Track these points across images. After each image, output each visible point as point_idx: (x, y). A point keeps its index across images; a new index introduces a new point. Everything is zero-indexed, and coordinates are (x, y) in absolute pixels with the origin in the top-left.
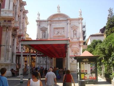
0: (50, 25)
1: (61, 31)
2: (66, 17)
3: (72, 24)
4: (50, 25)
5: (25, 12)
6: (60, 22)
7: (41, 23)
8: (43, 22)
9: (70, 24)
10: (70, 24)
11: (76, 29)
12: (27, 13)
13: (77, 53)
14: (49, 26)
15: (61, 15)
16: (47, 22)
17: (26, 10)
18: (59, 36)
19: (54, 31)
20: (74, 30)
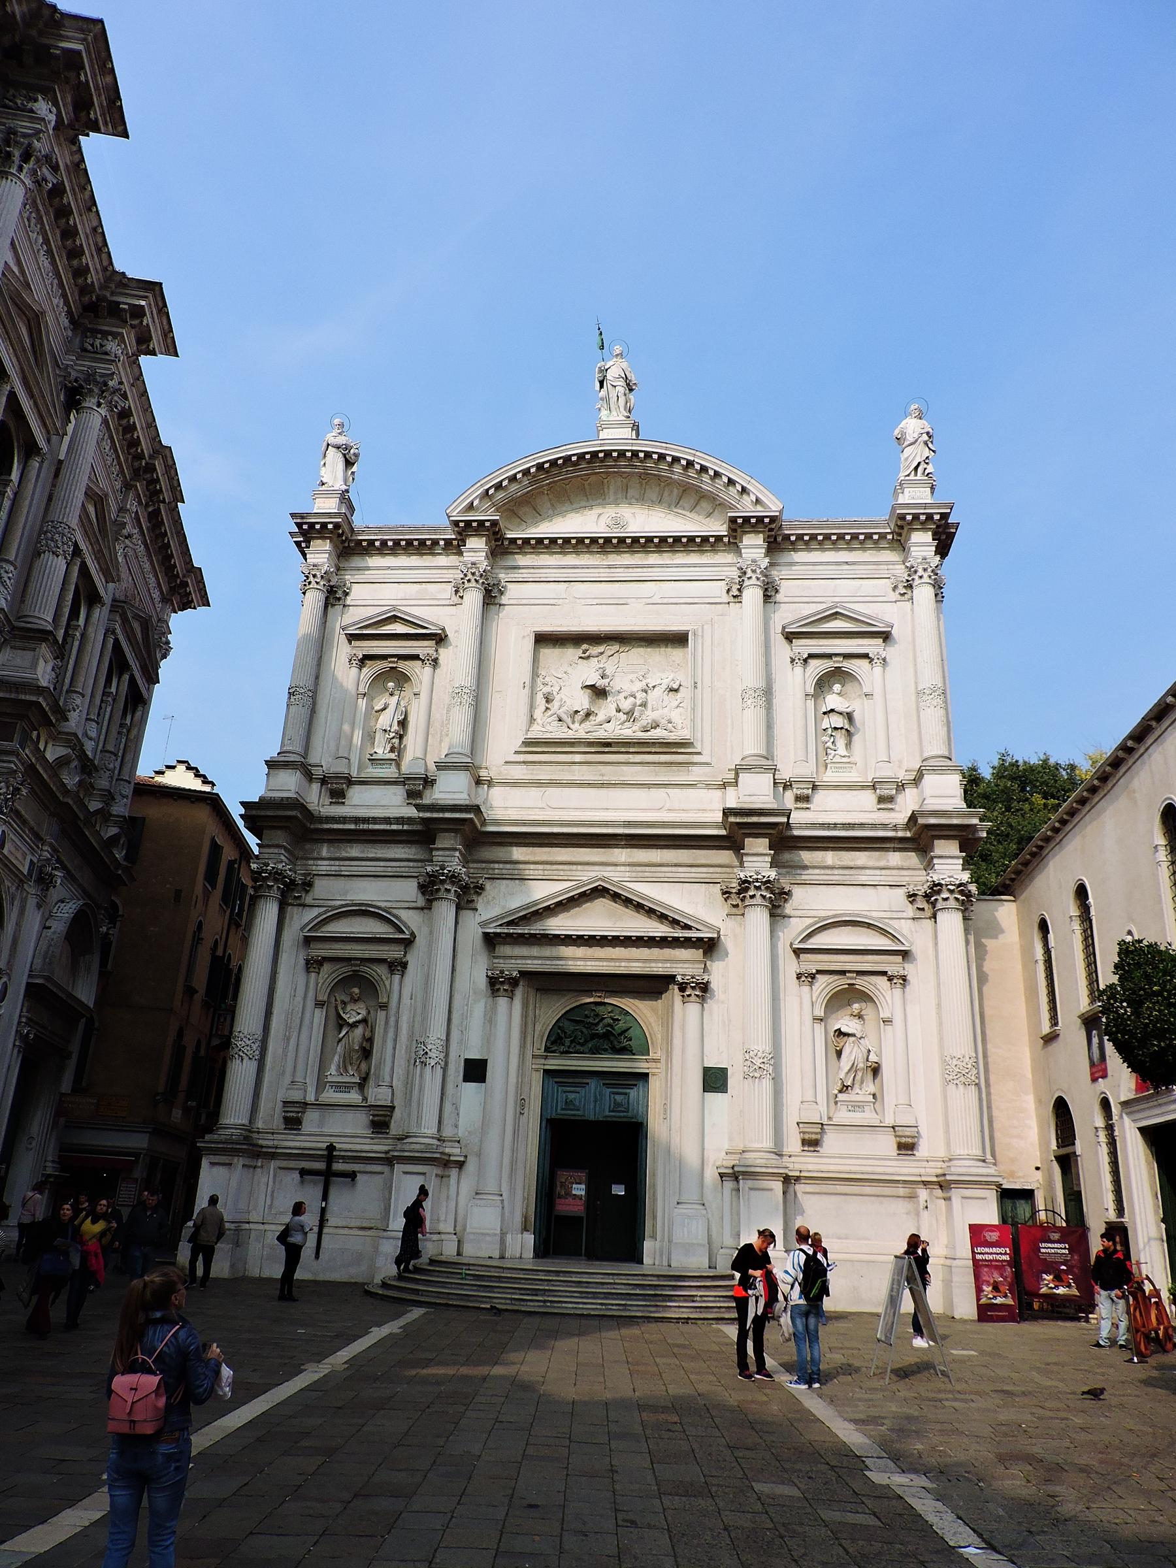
0: (491, 596)
1: (627, 671)
2: (716, 504)
3: (787, 589)
4: (491, 596)
5: (114, 310)
6: (627, 559)
7: (357, 561)
8: (384, 548)
9: (769, 593)
10: (769, 593)
11: (857, 667)
12: (144, 345)
13: (866, 997)
14: (473, 597)
15: (645, 478)
16: (442, 560)
17: (123, 282)
18: (606, 745)
19: (535, 674)
20: (818, 667)
